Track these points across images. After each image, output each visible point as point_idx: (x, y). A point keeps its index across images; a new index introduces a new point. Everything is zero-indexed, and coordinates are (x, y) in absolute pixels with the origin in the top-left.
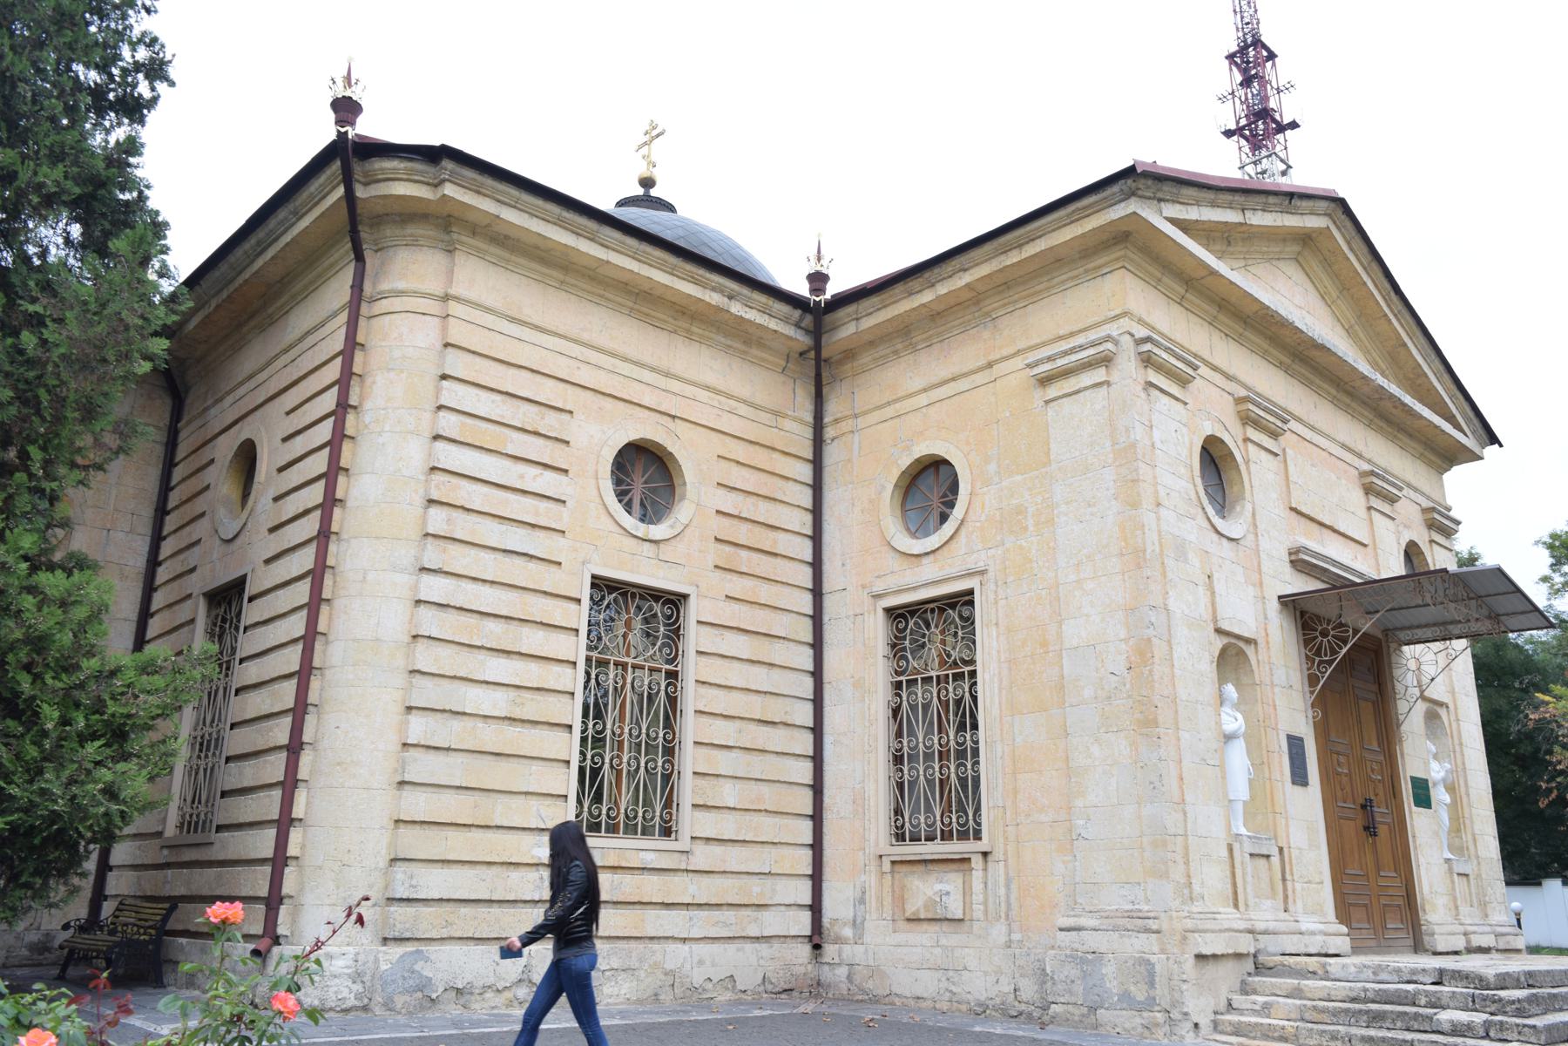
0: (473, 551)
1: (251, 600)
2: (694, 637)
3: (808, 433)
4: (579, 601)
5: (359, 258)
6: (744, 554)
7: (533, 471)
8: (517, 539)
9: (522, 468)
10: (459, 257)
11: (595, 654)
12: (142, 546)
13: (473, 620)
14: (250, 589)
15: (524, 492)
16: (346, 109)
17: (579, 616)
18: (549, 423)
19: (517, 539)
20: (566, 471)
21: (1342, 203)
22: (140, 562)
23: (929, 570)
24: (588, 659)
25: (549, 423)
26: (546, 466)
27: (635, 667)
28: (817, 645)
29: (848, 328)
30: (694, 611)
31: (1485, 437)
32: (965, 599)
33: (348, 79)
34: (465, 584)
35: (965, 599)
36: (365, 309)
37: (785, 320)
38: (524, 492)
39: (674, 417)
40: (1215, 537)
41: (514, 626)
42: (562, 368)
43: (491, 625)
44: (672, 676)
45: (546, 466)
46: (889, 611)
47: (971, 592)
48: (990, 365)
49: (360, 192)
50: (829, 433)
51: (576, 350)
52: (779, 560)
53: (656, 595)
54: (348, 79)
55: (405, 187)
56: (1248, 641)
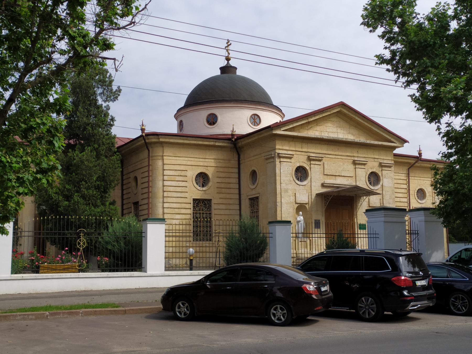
0: (172, 198)
1: (140, 206)
2: (214, 206)
3: (237, 162)
4: (191, 203)
5: (149, 151)
6: (223, 189)
7: (181, 182)
8: (179, 195)
9: (179, 182)
10: (164, 148)
11: (195, 212)
12: (120, 191)
13: (173, 209)
14: (140, 204)
15: (180, 187)
16: (143, 130)
17: (191, 206)
18: (183, 173)
19: (179, 195)
20: (187, 181)
21: (342, 104)
22: (120, 195)
23: (254, 192)
24: (193, 213)
25: (183, 173)
26: (183, 181)
27: (203, 213)
28: (240, 204)
29: (241, 143)
30: (213, 202)
31: (402, 141)
32: (257, 198)
33: (143, 125)
34: (171, 204)
35: (257, 198)
36: (151, 158)
37: (228, 143)
38: (180, 187)
39: (207, 166)
40: (298, 186)
41: (180, 209)
42: (184, 163)
43: (176, 210)
44: (210, 214)
45: (183, 181)
46: (250, 199)
47: (258, 197)
48: (260, 154)
49: (147, 141)
50: (241, 162)
51: (187, 159)
52: (231, 189)
53: (206, 200)
54: (143, 125)
55: (154, 140)
56: (306, 204)
